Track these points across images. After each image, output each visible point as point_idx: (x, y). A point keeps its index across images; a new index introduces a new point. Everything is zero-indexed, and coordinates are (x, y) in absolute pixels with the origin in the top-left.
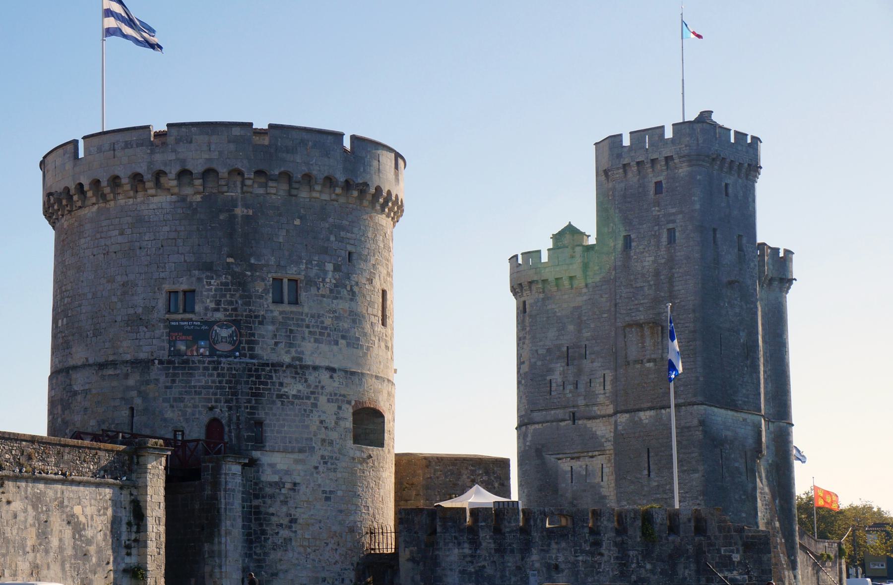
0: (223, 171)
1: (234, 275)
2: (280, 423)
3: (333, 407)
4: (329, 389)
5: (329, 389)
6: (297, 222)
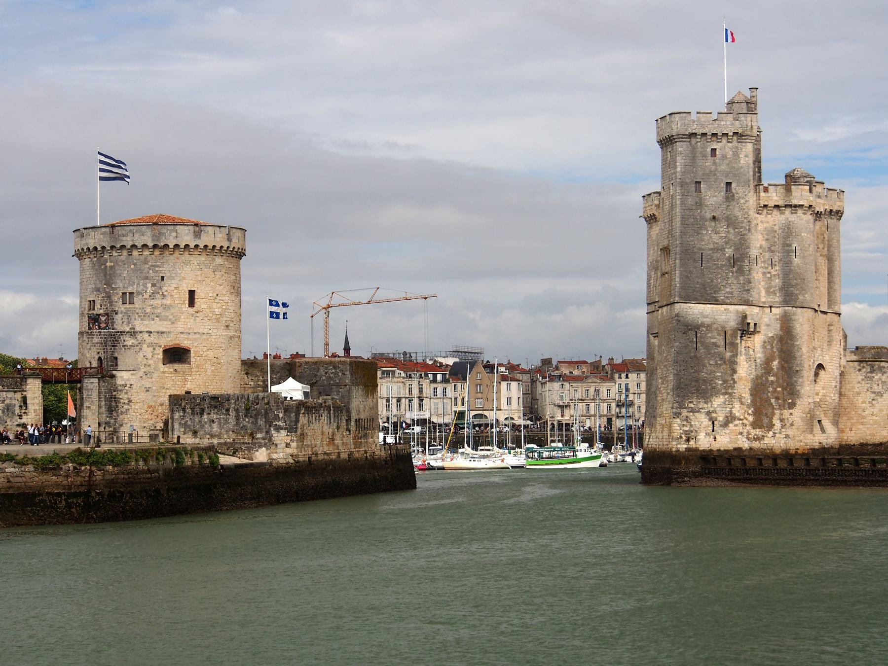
0: (99, 248)
1: (106, 292)
2: (125, 358)
3: (151, 349)
4: (147, 341)
5: (147, 341)
6: (132, 266)
